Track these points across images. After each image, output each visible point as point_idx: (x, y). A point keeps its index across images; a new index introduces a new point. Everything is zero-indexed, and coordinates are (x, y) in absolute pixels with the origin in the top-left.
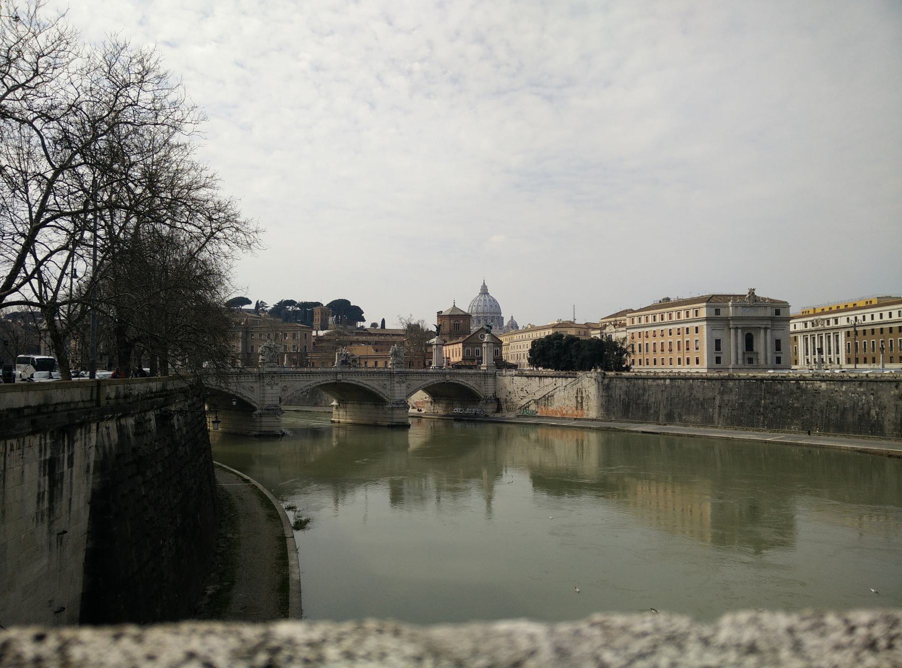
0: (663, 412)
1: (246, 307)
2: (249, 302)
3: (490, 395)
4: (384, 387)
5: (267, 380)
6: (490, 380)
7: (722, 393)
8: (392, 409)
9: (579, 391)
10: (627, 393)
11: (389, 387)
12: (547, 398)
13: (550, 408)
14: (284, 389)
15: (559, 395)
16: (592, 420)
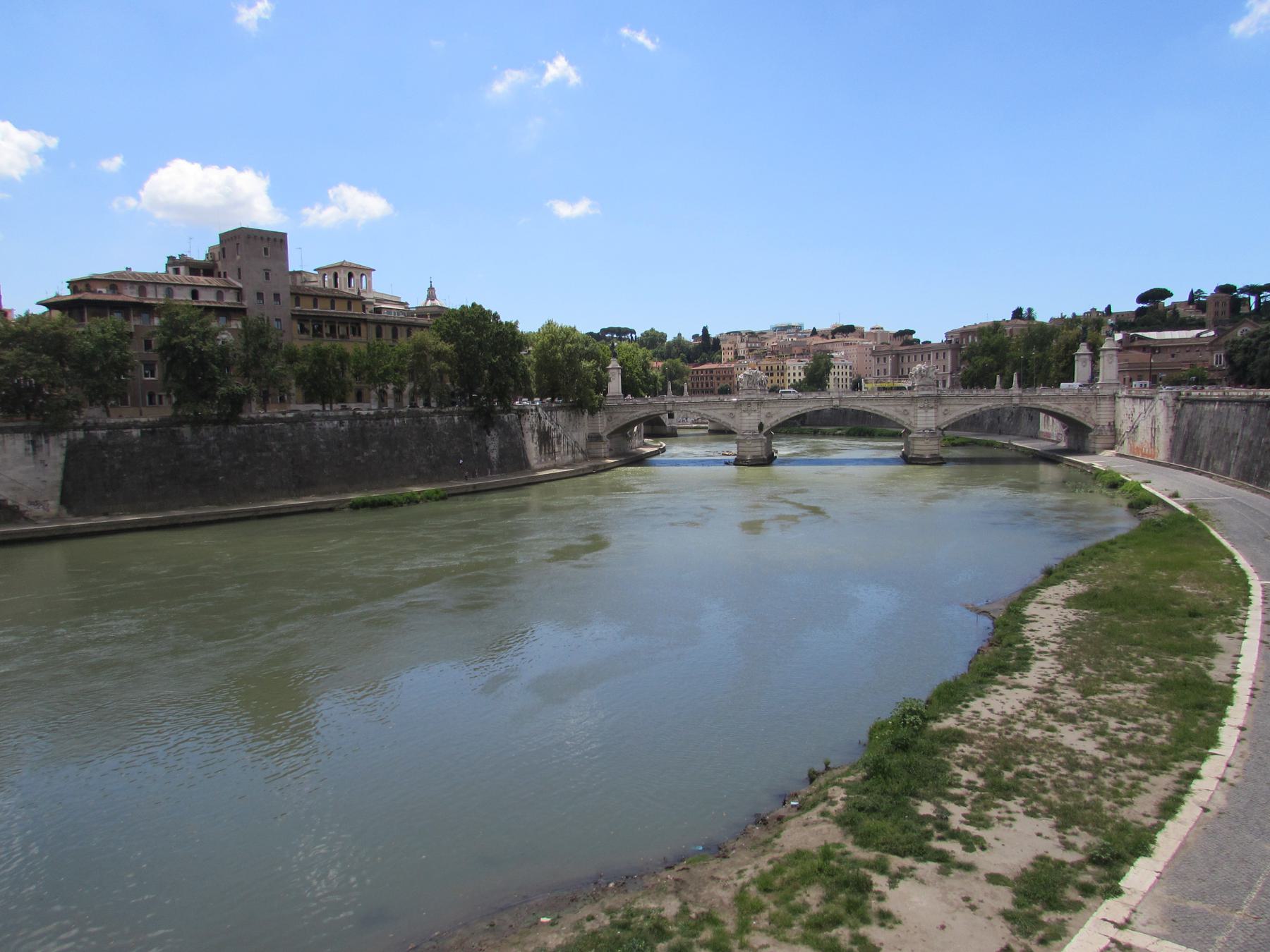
0: (1205, 454)
1: (1167, 302)
2: (1169, 294)
3: (1104, 422)
4: (906, 413)
5: (744, 408)
6: (1105, 404)
7: (1244, 425)
8: (914, 439)
9: (1154, 421)
10: (1189, 425)
11: (912, 413)
12: (1134, 429)
13: (1137, 444)
14: (769, 416)
15: (1144, 425)
16: (1159, 464)
